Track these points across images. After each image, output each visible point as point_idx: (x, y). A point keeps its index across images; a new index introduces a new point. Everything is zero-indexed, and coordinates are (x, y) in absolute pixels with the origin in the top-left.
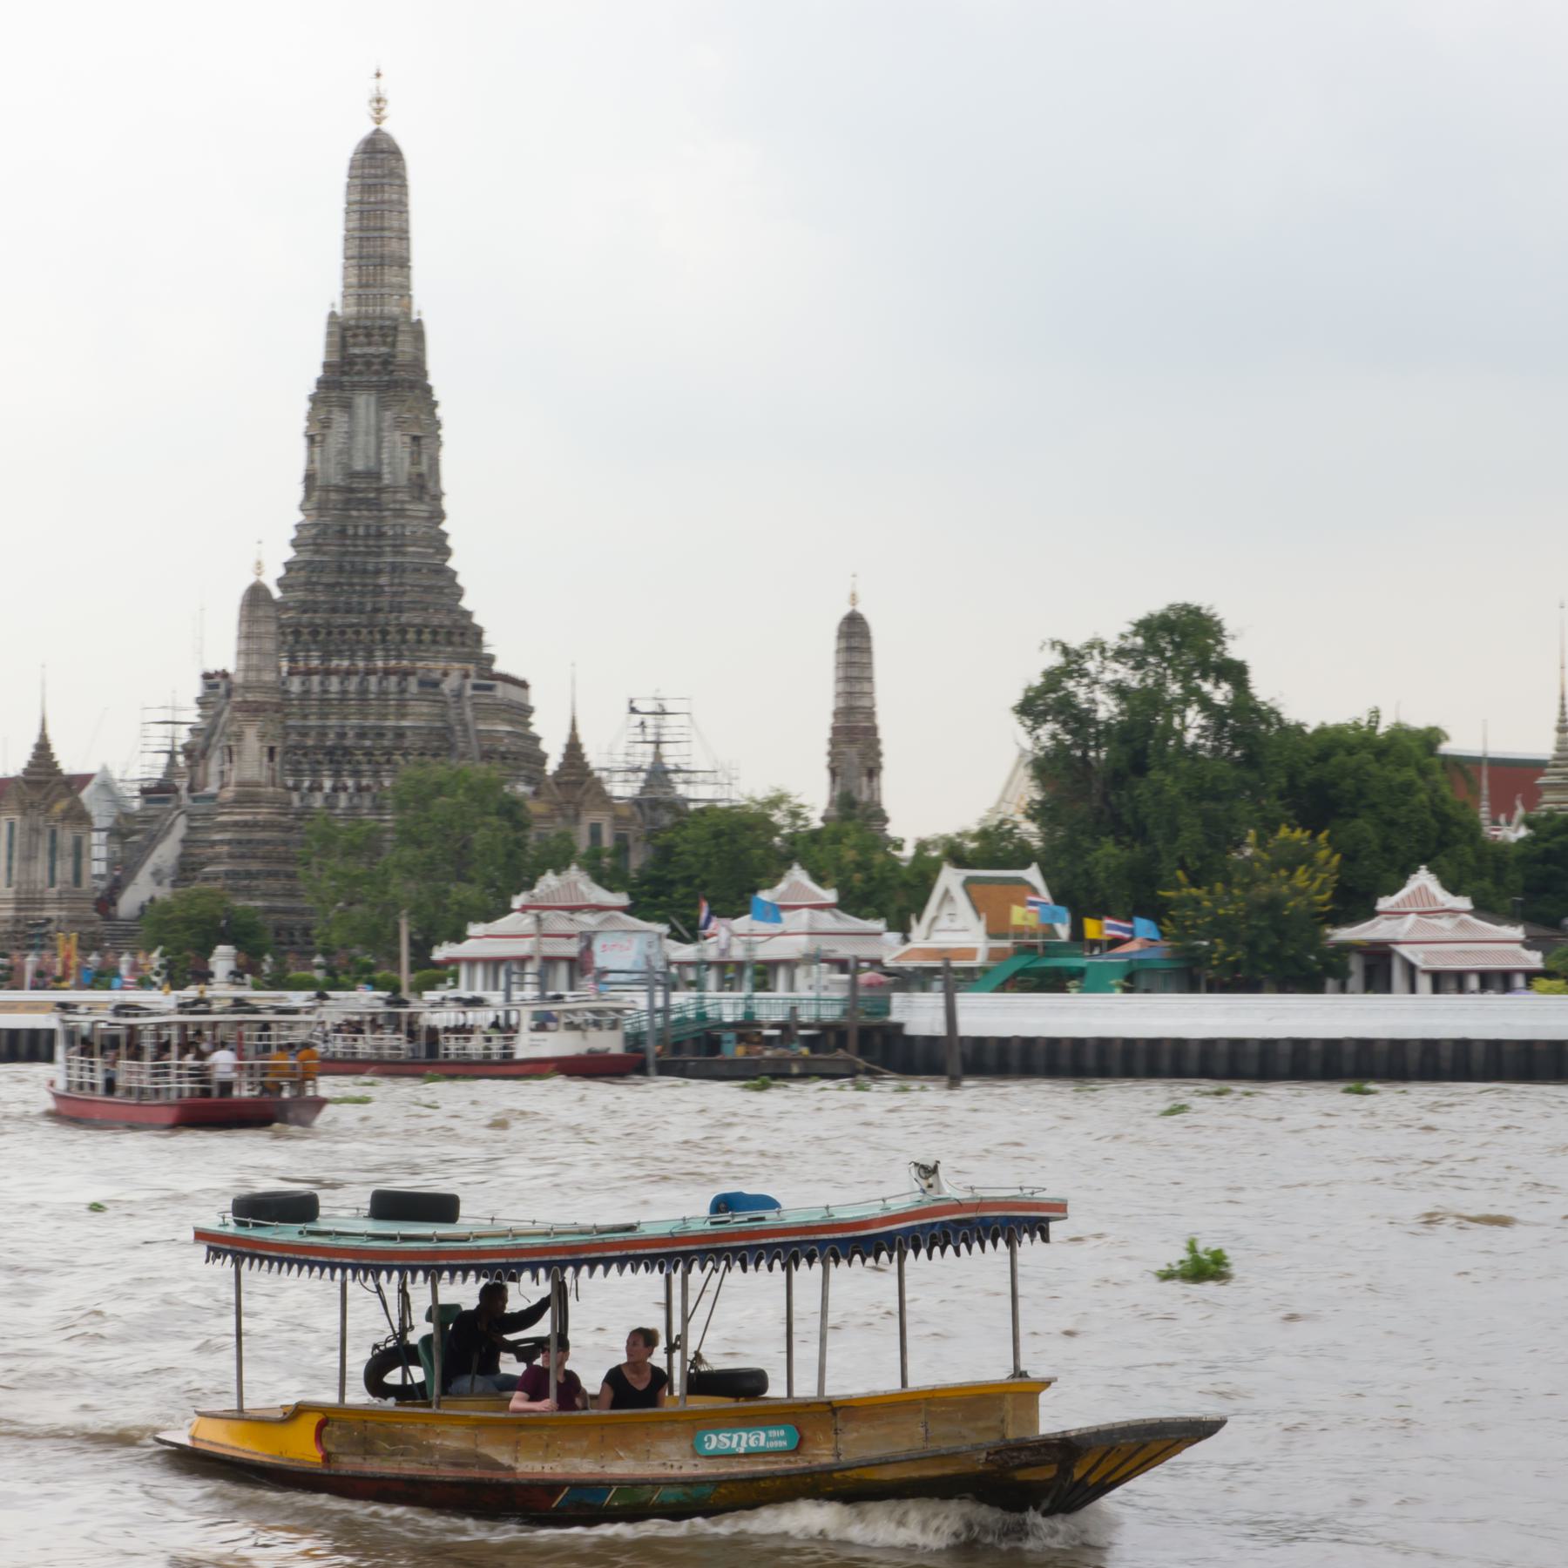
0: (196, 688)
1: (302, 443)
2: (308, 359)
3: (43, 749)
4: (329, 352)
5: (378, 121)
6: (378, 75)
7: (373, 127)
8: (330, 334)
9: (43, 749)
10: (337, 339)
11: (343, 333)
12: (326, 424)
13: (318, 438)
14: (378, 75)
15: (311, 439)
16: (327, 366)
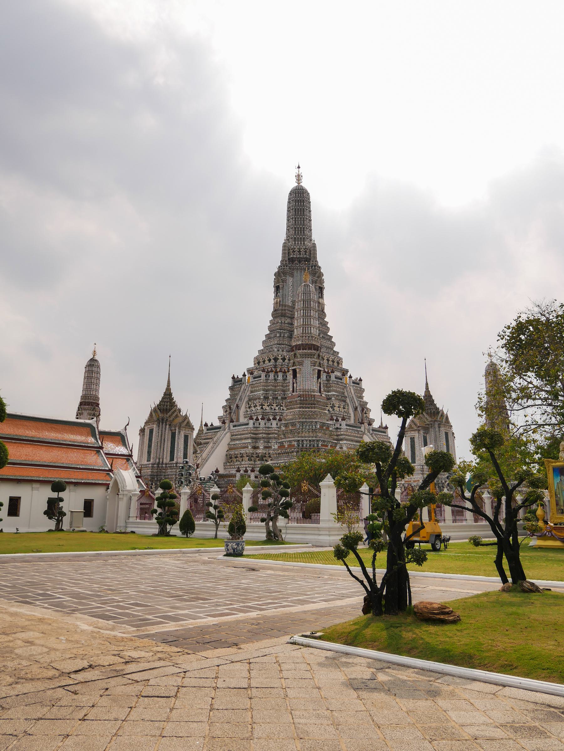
0: (230, 383)
1: (273, 289)
2: (275, 259)
3: (168, 395)
4: (283, 257)
5: (299, 183)
6: (299, 167)
7: (296, 184)
8: (283, 250)
9: (168, 395)
10: (287, 252)
11: (287, 250)
12: (284, 281)
13: (281, 286)
14: (299, 167)
15: (277, 288)
16: (282, 261)
